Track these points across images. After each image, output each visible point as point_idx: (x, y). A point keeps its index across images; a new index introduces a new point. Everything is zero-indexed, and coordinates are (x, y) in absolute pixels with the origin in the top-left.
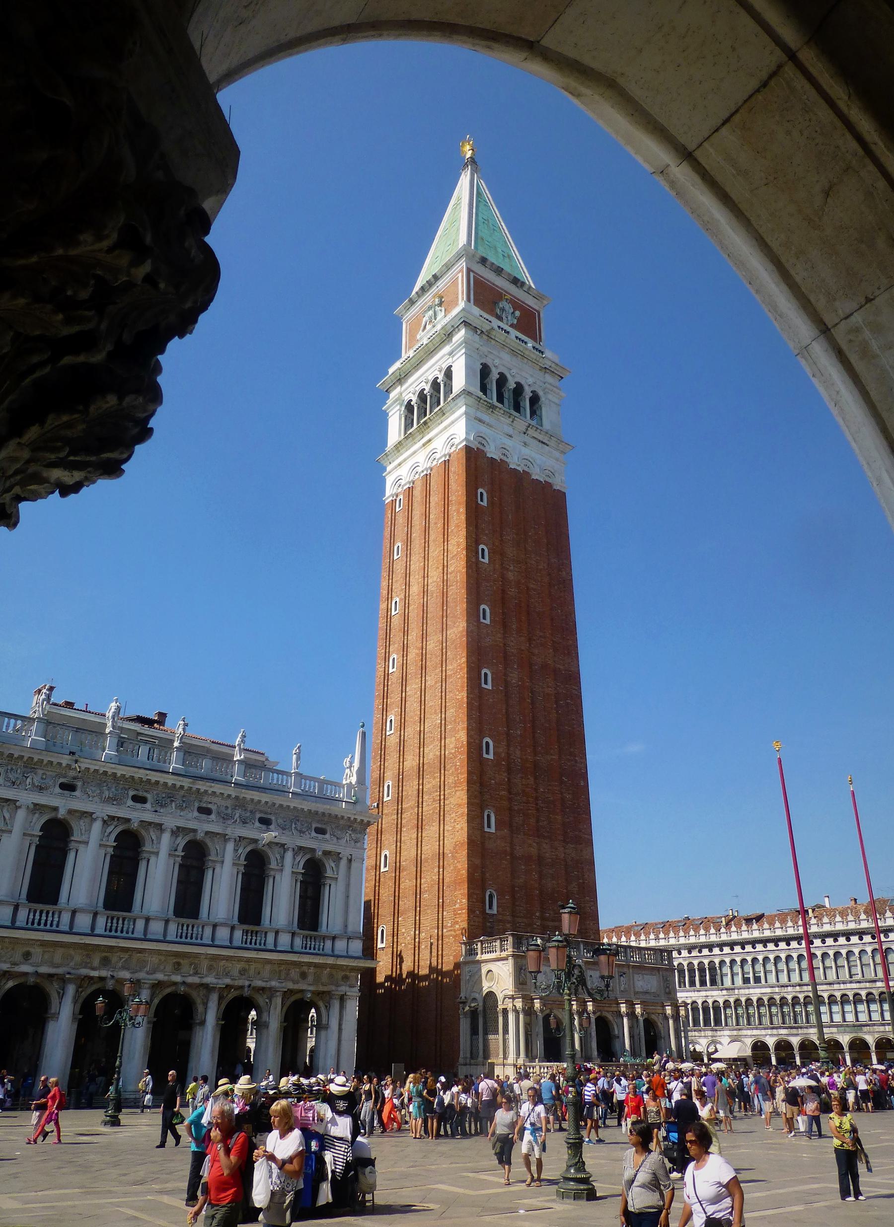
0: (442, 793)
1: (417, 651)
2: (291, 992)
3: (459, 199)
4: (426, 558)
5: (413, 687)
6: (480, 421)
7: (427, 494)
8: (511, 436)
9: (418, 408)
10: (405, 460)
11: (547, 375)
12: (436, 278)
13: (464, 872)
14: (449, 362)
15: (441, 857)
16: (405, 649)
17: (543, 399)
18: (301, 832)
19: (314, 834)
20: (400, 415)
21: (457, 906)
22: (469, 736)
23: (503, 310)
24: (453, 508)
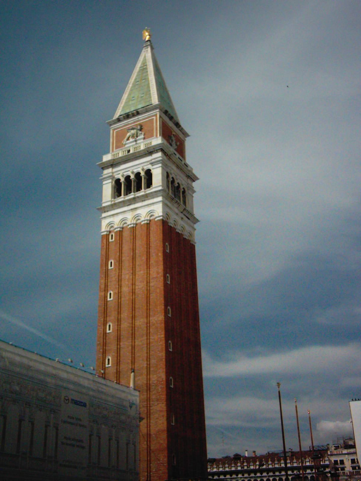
0: (148, 403)
1: (128, 325)
3: (144, 65)
4: (134, 273)
5: (126, 344)
6: (167, 205)
7: (134, 238)
9: (124, 184)
10: (117, 214)
11: (189, 179)
12: (138, 113)
13: (165, 445)
14: (150, 167)
15: (149, 436)
16: (119, 321)
17: (187, 193)
23: (172, 141)
24: (152, 251)
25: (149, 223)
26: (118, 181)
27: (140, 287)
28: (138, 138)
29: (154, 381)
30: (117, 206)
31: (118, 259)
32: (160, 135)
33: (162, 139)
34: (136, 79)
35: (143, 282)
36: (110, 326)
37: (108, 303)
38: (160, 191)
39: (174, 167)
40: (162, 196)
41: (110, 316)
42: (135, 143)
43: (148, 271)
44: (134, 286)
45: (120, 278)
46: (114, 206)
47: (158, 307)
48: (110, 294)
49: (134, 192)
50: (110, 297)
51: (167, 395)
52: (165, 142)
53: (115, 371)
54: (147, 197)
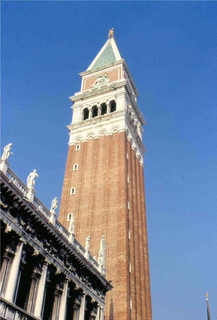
1: (89, 213)
7: (98, 147)
10: (84, 130)
14: (113, 99)
20: (81, 112)
25: (112, 136)
27: (102, 183)
29: (113, 263)
37: (70, 197)
41: (71, 208)
43: (110, 171)
45: (83, 177)
54: (112, 117)
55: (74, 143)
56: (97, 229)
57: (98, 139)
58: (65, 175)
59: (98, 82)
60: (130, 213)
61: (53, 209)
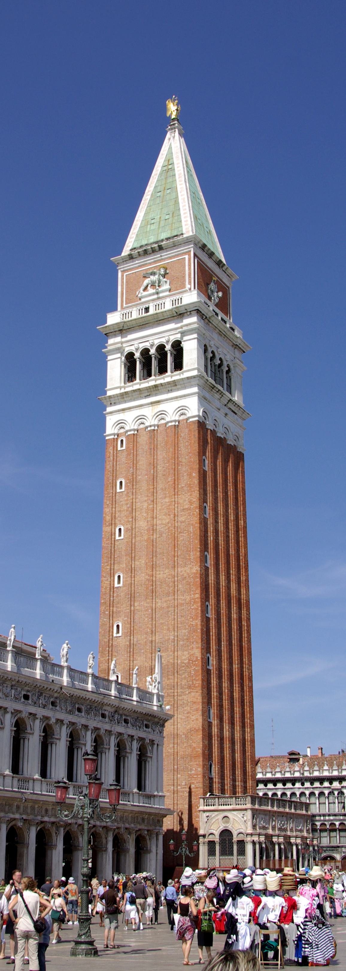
0: (176, 691)
1: (147, 577)
2: (140, 830)
3: (169, 162)
8: (219, 410)
10: (130, 408)
12: (161, 248)
13: (200, 750)
14: (178, 337)
15: (176, 736)
17: (232, 371)
18: (140, 727)
19: (145, 728)
20: (121, 362)
21: (193, 772)
22: (202, 654)
24: (183, 469)
26: (130, 357)
27: (164, 522)
28: (160, 290)
29: (185, 660)
30: (129, 397)
31: (130, 478)
32: (195, 288)
33: (198, 295)
34: (156, 187)
35: (169, 515)
36: (119, 577)
38: (194, 377)
39: (215, 336)
40: (199, 386)
41: (119, 563)
42: (156, 296)
43: (176, 500)
44: (155, 520)
45: (134, 507)
46: (124, 396)
47: (192, 553)
48: (120, 530)
49: (155, 376)
50: (120, 535)
51: (203, 680)
52: (204, 299)
53: (128, 643)
54: (176, 385)
55: (114, 434)
56: (159, 604)
57: (154, 430)
58: (105, 501)
59: (150, 285)
60: (212, 571)
61: (90, 667)
